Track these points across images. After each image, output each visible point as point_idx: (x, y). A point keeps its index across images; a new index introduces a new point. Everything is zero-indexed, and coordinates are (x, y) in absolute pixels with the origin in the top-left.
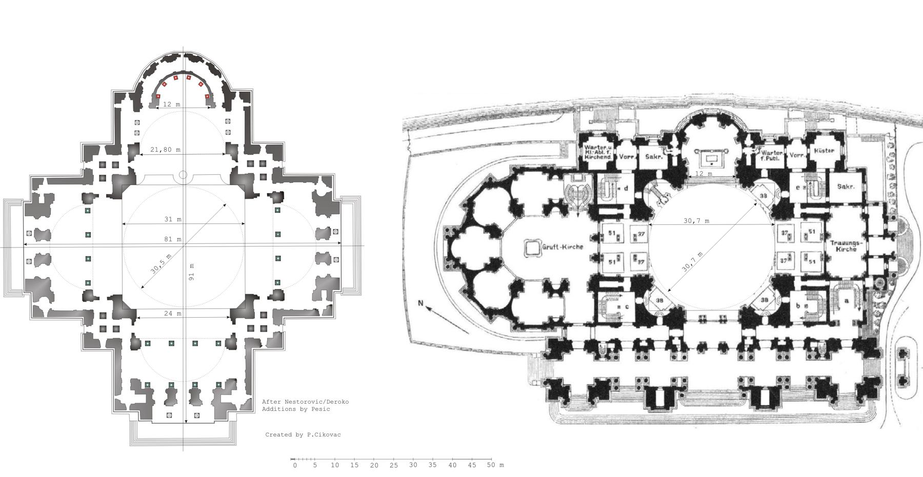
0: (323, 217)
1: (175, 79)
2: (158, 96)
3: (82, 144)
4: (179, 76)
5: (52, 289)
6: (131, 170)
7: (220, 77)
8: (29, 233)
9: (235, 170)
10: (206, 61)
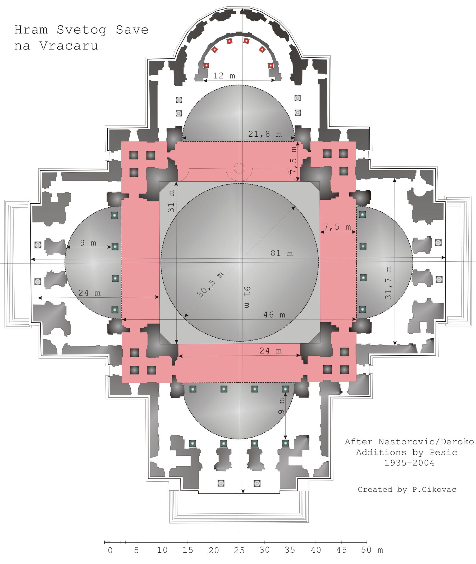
0: (422, 223)
1: (228, 43)
2: (206, 65)
3: (107, 127)
4: (234, 38)
5: (68, 318)
6: (171, 162)
7: (287, 40)
8: (38, 245)
9: (307, 161)
10: (269, 19)
